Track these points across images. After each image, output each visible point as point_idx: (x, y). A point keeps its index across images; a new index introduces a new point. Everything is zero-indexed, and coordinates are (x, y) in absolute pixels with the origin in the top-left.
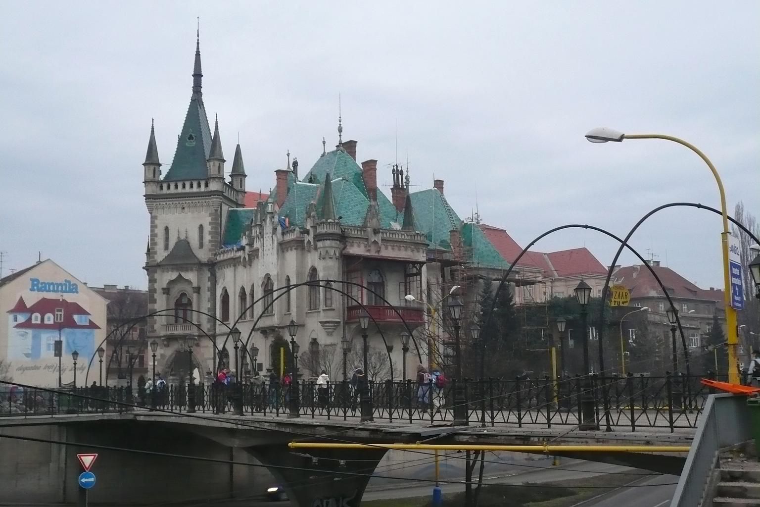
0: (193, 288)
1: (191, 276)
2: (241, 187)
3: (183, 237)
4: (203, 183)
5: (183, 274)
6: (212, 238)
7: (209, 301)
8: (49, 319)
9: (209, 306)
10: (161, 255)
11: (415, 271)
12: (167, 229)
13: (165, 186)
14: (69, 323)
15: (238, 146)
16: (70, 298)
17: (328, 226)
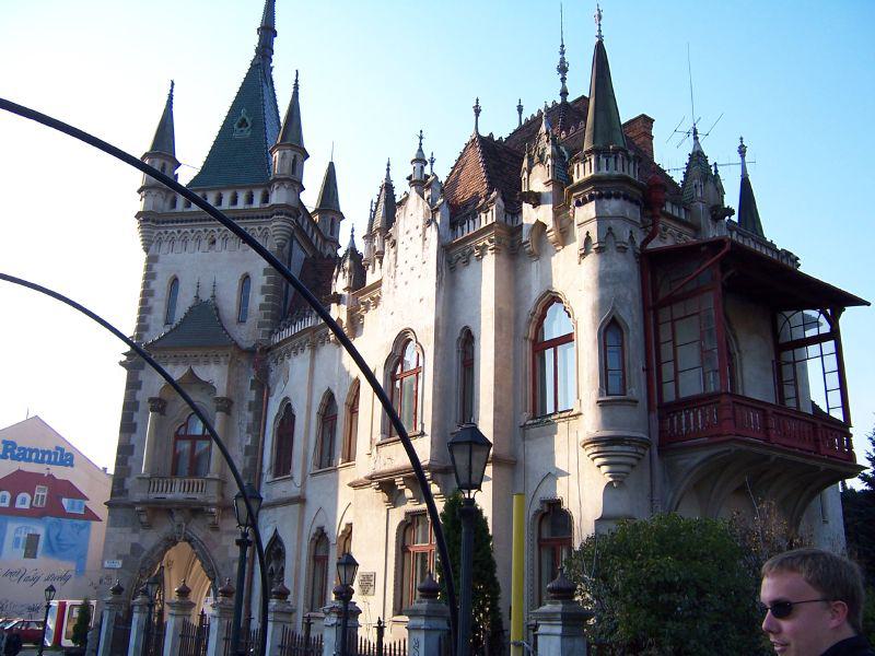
0: (217, 399)
1: (214, 374)
2: (332, 234)
3: (206, 297)
8: (24, 501)
9: (249, 443)
12: (175, 281)
14: (52, 509)
15: (331, 164)
16: (60, 473)
17: (612, 161)
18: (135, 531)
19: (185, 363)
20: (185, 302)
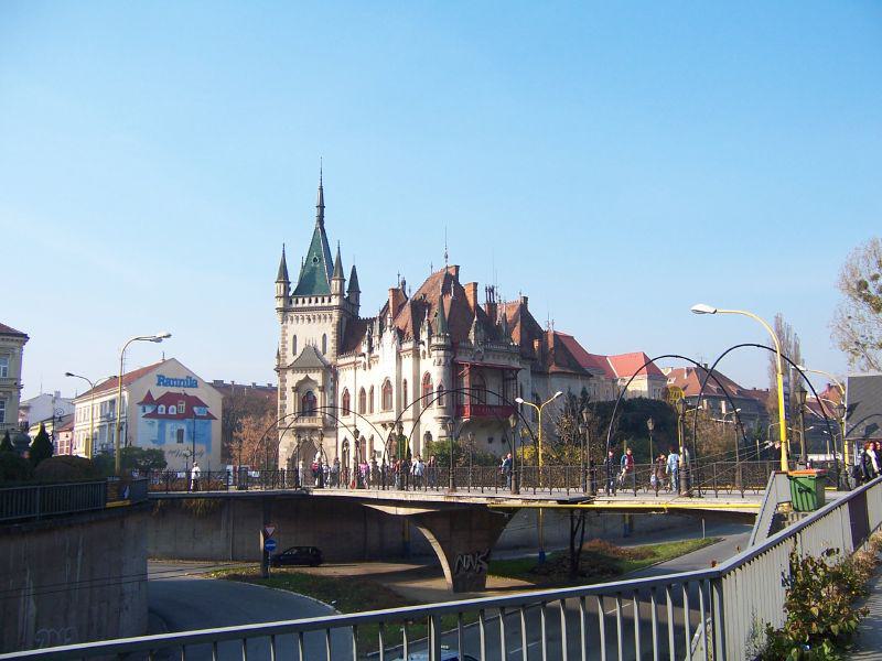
4: (326, 299)
8: (173, 410)
10: (290, 360)
11: (511, 376)
13: (294, 300)
14: (189, 414)
16: (191, 392)
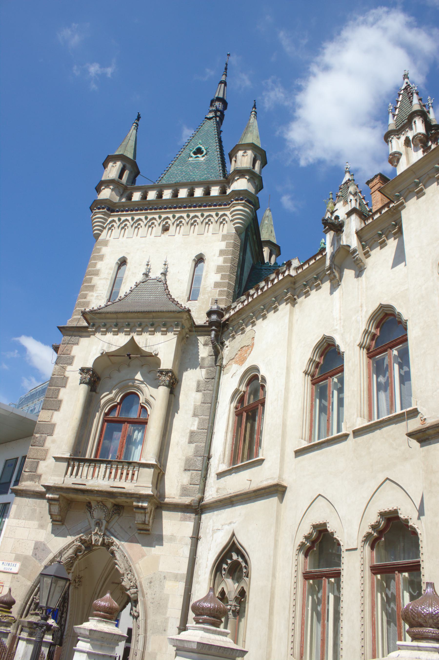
1: (163, 346)
5: (137, 338)
6: (222, 278)
7: (195, 415)
12: (123, 262)
18: (42, 526)
19: (127, 333)
20: (132, 278)
